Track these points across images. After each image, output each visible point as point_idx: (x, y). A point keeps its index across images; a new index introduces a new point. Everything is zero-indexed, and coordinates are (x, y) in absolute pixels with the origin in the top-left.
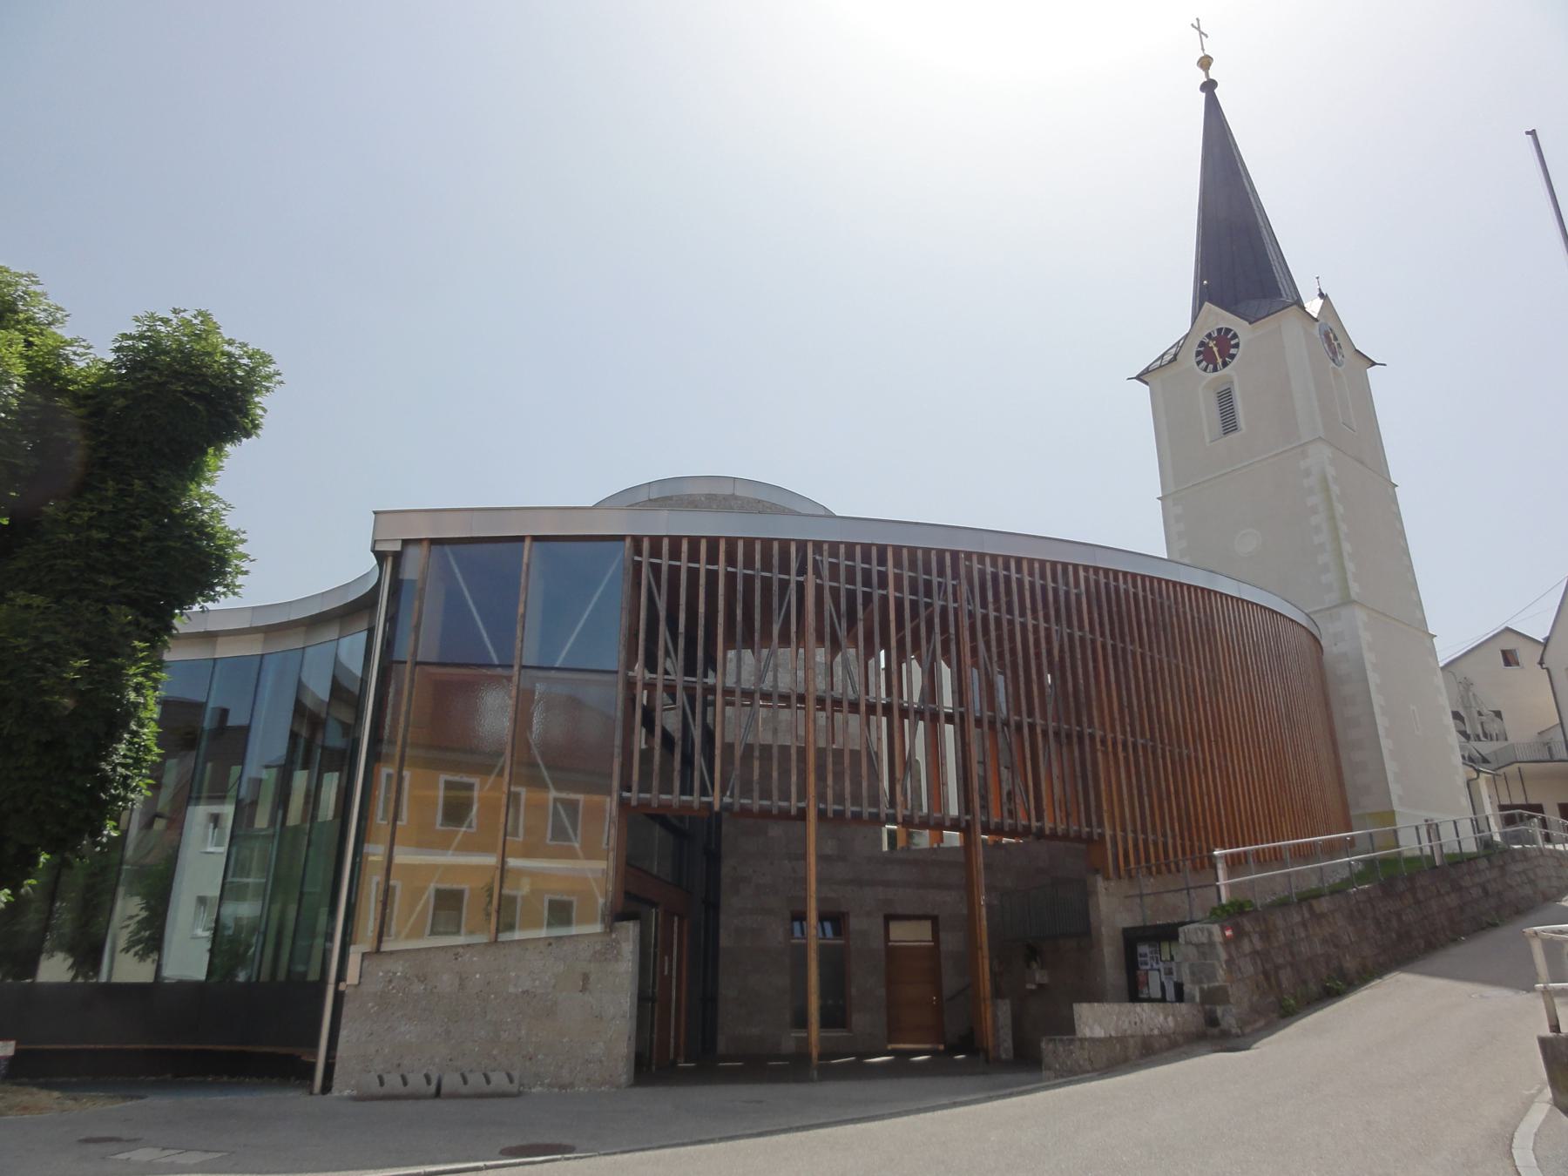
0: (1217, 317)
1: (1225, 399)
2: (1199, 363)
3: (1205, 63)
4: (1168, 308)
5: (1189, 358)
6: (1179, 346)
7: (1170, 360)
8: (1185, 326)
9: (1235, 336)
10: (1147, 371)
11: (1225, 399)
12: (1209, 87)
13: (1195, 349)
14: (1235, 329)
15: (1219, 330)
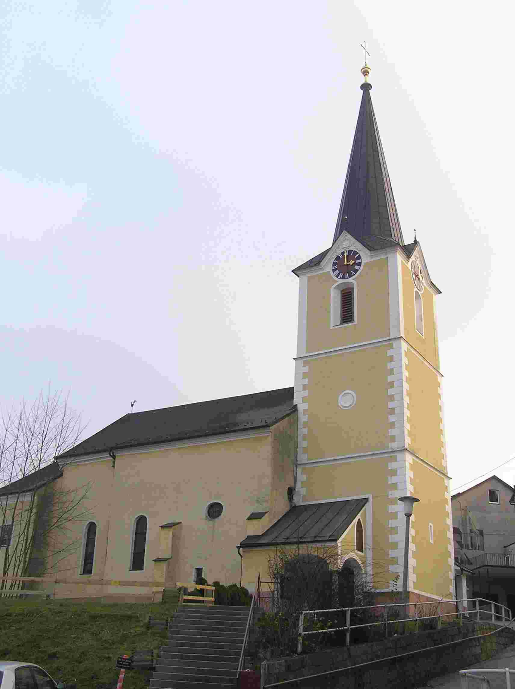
0: (350, 243)
1: (347, 297)
2: (334, 270)
3: (365, 72)
4: (318, 229)
5: (328, 266)
6: (323, 255)
7: (315, 262)
8: (329, 244)
9: (359, 258)
10: (301, 268)
11: (347, 297)
12: (366, 87)
13: (333, 261)
14: (361, 254)
15: (350, 251)
